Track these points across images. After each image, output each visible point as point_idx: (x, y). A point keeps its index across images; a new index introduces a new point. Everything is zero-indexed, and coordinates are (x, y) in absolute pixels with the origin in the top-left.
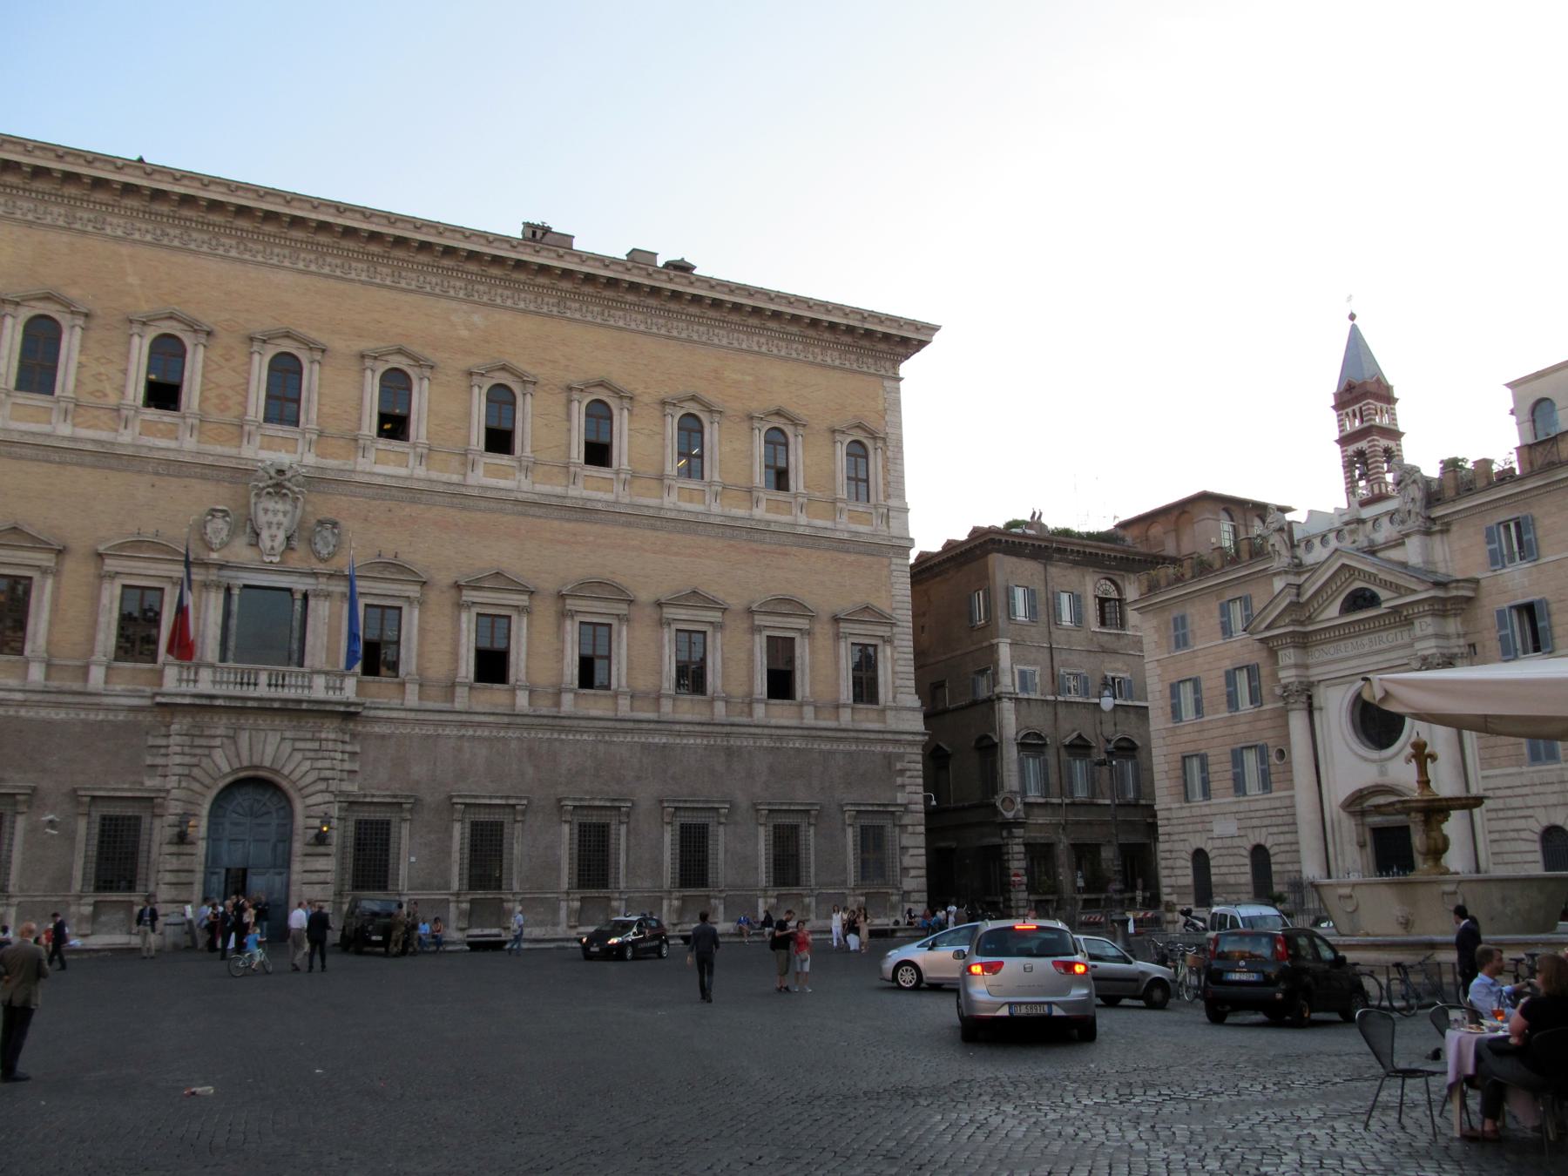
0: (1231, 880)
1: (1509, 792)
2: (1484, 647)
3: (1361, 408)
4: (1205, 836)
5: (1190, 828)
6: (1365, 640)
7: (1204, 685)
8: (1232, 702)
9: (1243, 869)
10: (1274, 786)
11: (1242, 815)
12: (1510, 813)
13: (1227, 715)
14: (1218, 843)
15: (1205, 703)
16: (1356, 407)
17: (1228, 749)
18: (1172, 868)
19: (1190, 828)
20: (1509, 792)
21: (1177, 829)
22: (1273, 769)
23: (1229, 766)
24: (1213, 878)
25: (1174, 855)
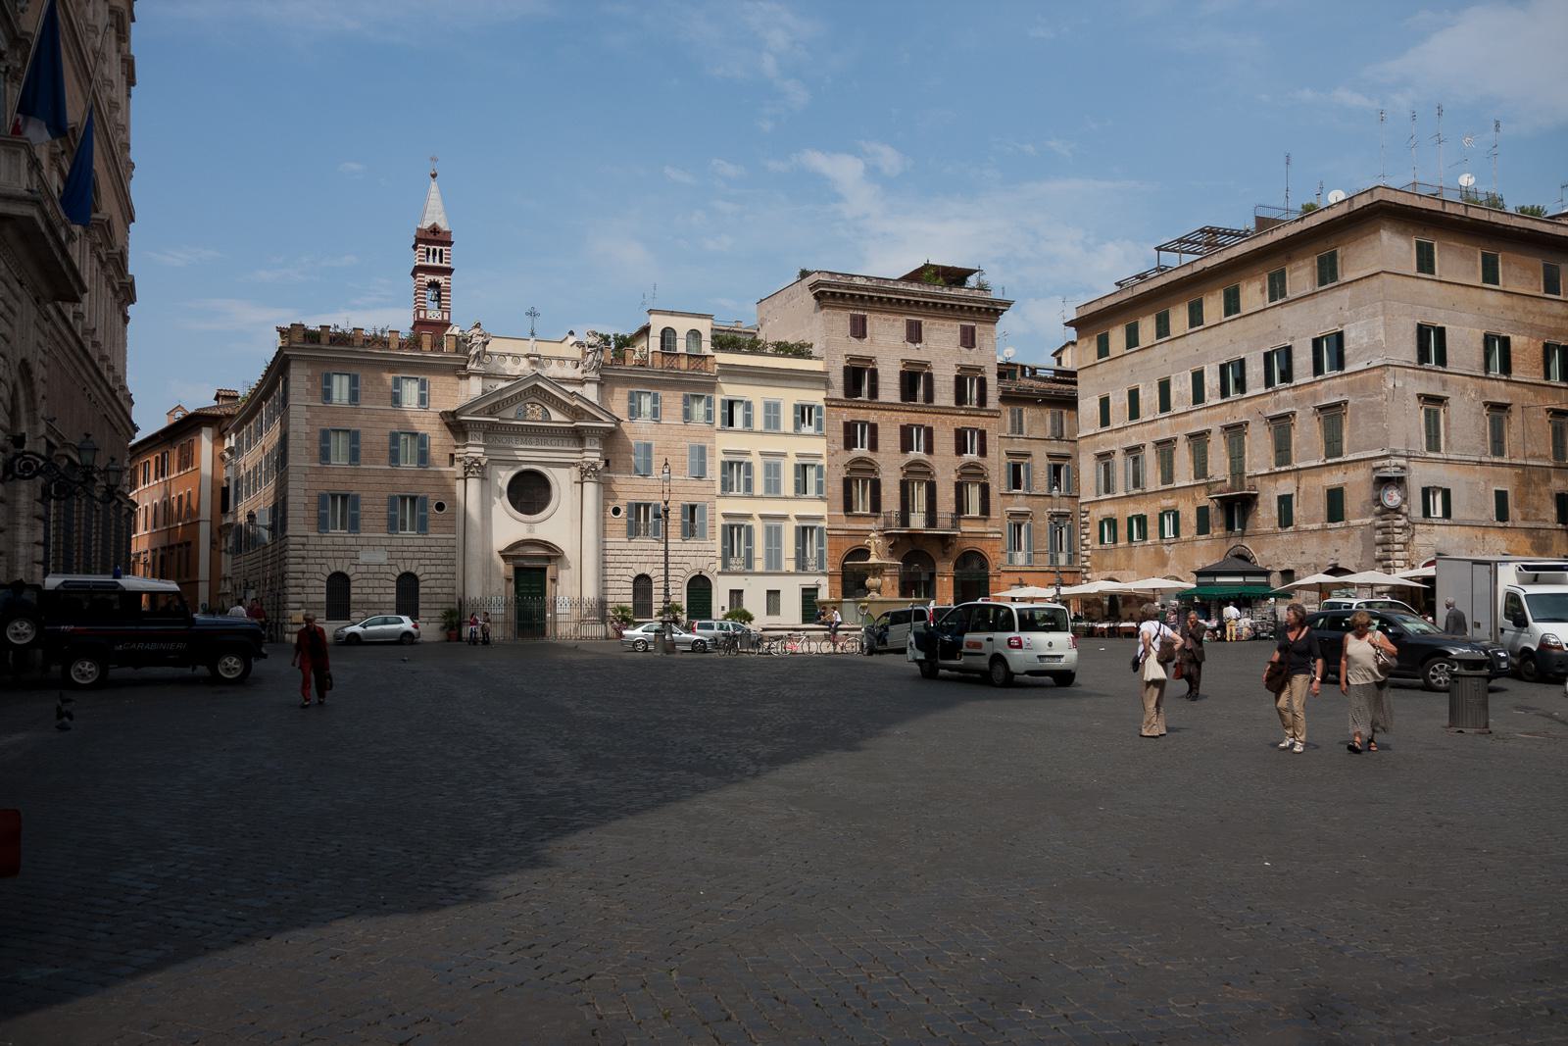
0: (375, 598)
1: (619, 552)
2: (615, 463)
3: (441, 251)
4: (347, 561)
5: (330, 554)
6: (534, 439)
7: (362, 439)
8: (394, 458)
9: (388, 591)
10: (430, 530)
11: (395, 549)
12: (618, 565)
13: (388, 467)
14: (363, 569)
15: (362, 454)
16: (438, 248)
17: (386, 495)
18: (303, 587)
19: (330, 554)
20: (619, 552)
21: (311, 554)
22: (431, 517)
23: (384, 509)
24: (353, 597)
25: (307, 575)
